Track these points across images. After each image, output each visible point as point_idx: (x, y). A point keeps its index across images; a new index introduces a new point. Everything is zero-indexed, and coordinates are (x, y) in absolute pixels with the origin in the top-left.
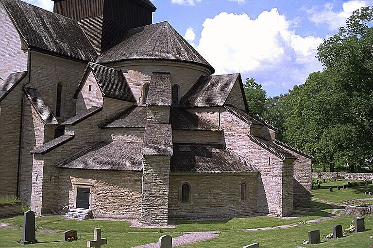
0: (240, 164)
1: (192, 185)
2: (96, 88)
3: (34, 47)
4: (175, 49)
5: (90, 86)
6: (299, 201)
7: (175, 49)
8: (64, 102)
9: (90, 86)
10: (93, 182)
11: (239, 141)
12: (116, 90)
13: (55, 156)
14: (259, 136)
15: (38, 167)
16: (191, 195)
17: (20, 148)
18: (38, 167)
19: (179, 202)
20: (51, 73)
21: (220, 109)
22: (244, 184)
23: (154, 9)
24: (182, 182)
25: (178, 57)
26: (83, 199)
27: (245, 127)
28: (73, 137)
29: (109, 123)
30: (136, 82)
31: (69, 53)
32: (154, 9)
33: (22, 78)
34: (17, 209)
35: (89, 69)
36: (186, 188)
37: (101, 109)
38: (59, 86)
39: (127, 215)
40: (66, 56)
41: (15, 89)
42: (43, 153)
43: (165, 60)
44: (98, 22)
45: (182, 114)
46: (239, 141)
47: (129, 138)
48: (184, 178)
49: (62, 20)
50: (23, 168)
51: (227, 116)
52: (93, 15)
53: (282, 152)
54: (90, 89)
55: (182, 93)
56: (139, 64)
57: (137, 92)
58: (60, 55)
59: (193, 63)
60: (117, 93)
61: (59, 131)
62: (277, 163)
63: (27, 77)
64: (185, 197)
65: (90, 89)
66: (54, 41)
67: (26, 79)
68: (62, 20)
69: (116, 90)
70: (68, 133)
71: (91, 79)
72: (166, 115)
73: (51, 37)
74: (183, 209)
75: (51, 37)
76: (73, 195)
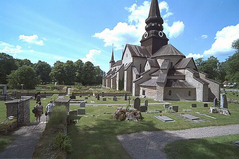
0: (189, 85)
2: (149, 65)
3: (134, 56)
6: (209, 96)
8: (141, 69)
10: (146, 89)
11: (190, 79)
12: (155, 66)
13: (138, 82)
14: (196, 77)
15: (134, 85)
16: (171, 93)
18: (134, 85)
20: (138, 62)
21: (184, 69)
22: (189, 92)
23: (169, 40)
26: (144, 94)
27: (191, 74)
28: (142, 78)
29: (152, 74)
30: (160, 62)
32: (169, 40)
34: (130, 94)
36: (170, 91)
37: (150, 70)
38: (141, 65)
39: (154, 97)
40: (142, 57)
45: (172, 71)
46: (190, 79)
47: (157, 78)
48: (169, 89)
49: (142, 47)
51: (186, 71)
53: (204, 82)
55: (174, 65)
56: (161, 57)
57: (160, 65)
58: (141, 57)
61: (140, 76)
62: (201, 86)
64: (170, 94)
68: (142, 47)
69: (155, 66)
70: (141, 77)
71: (148, 62)
72: (167, 71)
74: (169, 97)
76: (141, 91)
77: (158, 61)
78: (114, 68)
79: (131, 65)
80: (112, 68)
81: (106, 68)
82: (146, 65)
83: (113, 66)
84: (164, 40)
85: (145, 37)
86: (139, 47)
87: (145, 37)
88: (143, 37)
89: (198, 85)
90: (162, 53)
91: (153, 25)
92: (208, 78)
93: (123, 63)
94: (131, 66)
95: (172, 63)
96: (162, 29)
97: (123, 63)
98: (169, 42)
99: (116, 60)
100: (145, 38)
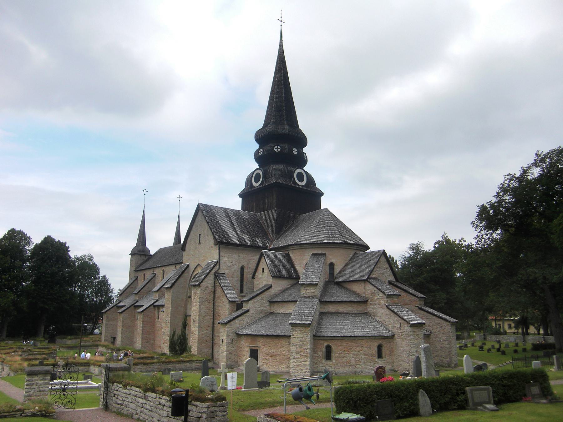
1: (334, 347)
2: (266, 271)
4: (330, 233)
5: (263, 269)
7: (330, 233)
9: (263, 269)
16: (333, 355)
17: (213, 319)
19: (324, 361)
22: (380, 347)
23: (322, 194)
24: (325, 344)
25: (331, 240)
30: (301, 261)
31: (249, 244)
32: (322, 194)
33: (214, 267)
35: (262, 255)
38: (242, 269)
40: (246, 246)
41: (209, 275)
42: (226, 323)
43: (321, 243)
44: (273, 213)
49: (246, 215)
50: (216, 334)
52: (269, 208)
54: (263, 271)
55: (337, 270)
59: (345, 243)
60: (284, 273)
63: (218, 265)
64: (328, 356)
65: (263, 271)
66: (237, 234)
67: (217, 267)
68: (246, 215)
73: (236, 232)
75: (236, 232)
77: (293, 258)
78: (149, 274)
79: (213, 271)
80: (140, 275)
81: (117, 275)
82: (260, 269)
83: (147, 265)
84: (310, 196)
85: (256, 182)
86: (236, 212)
87: (256, 182)
88: (249, 181)
89: (399, 326)
90: (305, 233)
91: (277, 149)
92: (426, 304)
93: (185, 263)
94: (211, 276)
95: (332, 265)
96: (302, 160)
97: (185, 263)
98: (325, 203)
99: (153, 247)
100: (256, 185)
